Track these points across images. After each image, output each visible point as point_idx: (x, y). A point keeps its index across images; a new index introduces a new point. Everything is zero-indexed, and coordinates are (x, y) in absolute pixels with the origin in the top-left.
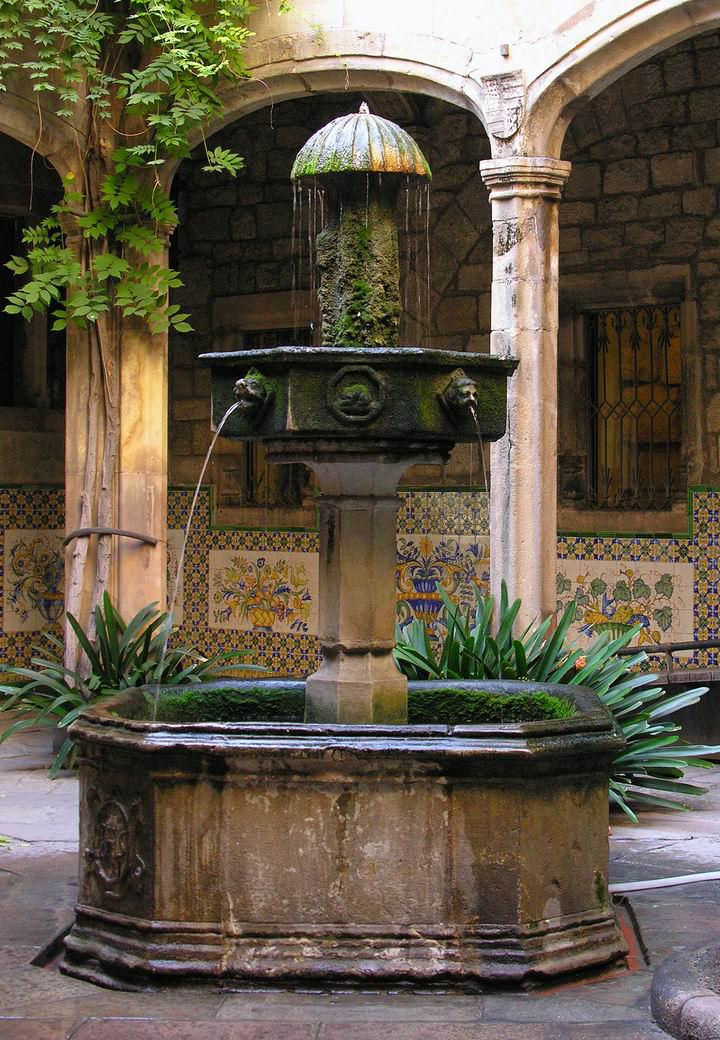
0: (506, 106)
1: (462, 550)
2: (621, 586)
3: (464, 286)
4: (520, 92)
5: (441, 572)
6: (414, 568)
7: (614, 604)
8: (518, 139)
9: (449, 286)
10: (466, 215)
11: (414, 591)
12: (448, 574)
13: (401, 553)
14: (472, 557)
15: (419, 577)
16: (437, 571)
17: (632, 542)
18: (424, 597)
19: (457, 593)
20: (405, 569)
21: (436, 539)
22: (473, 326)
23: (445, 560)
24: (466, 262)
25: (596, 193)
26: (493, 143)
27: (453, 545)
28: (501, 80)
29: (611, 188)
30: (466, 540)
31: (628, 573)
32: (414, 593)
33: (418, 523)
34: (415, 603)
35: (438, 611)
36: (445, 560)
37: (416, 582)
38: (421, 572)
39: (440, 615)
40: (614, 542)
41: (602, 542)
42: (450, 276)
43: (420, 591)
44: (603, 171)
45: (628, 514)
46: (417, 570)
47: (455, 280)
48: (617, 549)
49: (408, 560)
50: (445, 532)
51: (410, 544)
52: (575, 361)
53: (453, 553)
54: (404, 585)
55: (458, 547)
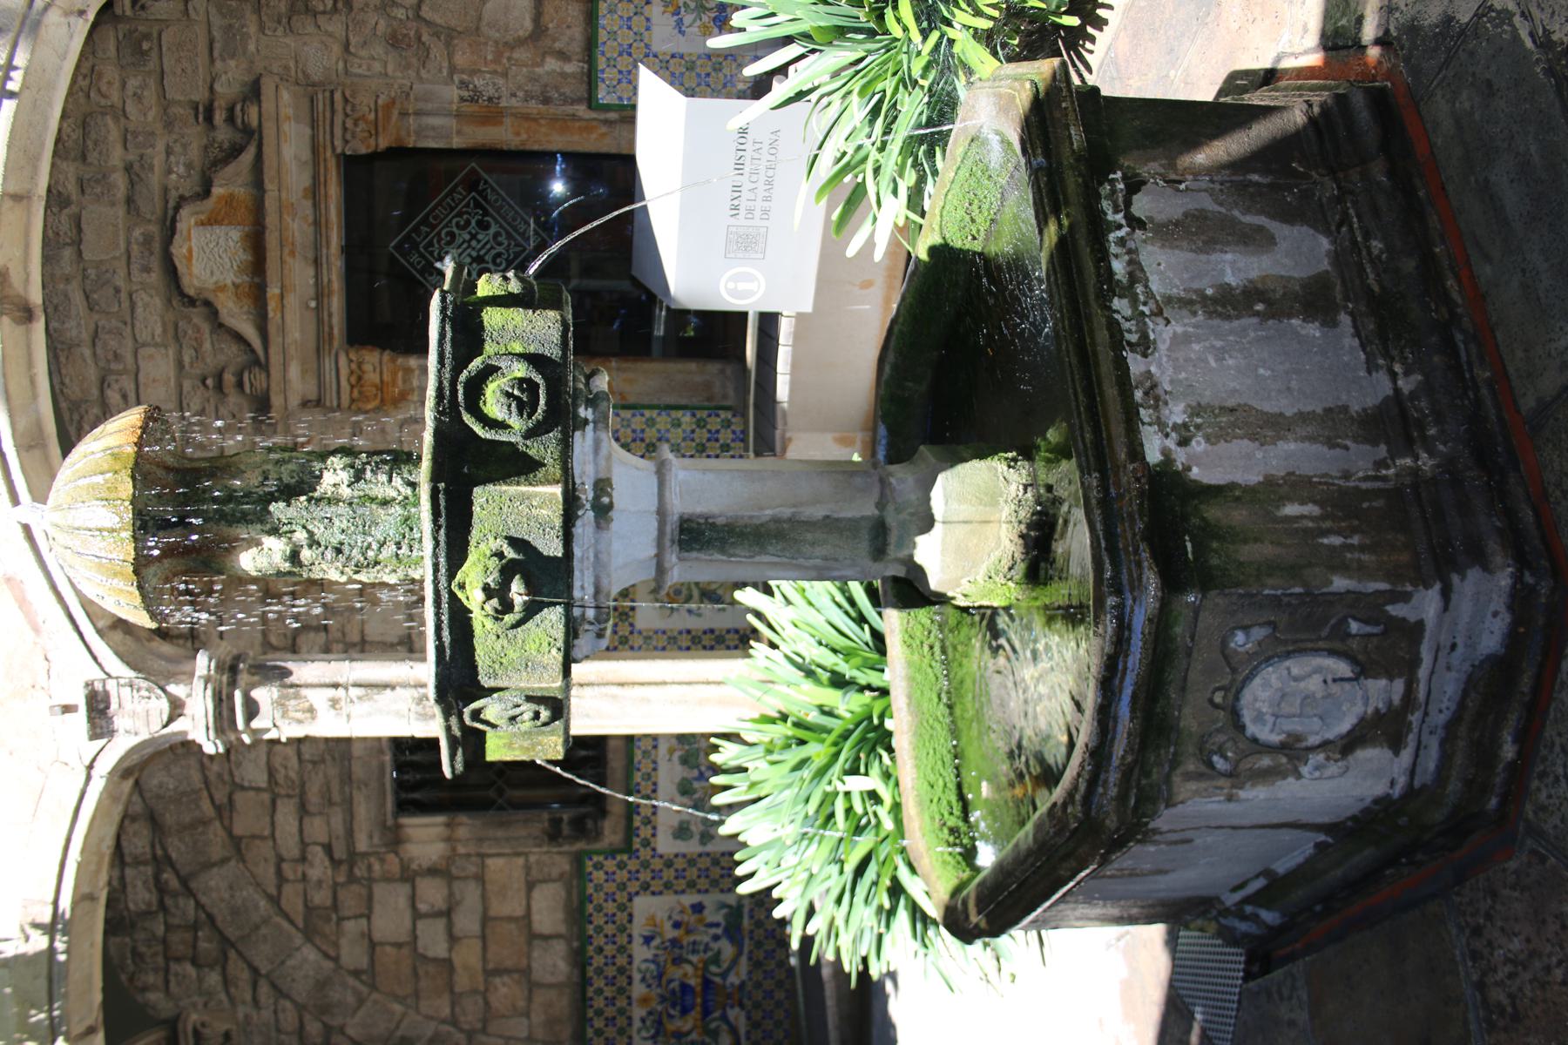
0: (128, 705)
1: (649, 955)
2: (684, 761)
3: (364, 962)
4: (111, 686)
7: (703, 768)
8: (172, 688)
9: (362, 982)
10: (283, 963)
11: (693, 1013)
12: (675, 973)
13: (652, 1031)
15: (678, 1008)
16: (672, 985)
17: (639, 748)
18: (699, 1000)
19: (694, 958)
20: (671, 1026)
21: (638, 990)
22: (406, 951)
23: (660, 976)
24: (336, 959)
25: (266, 797)
26: (175, 727)
28: (98, 709)
29: (261, 779)
30: (641, 953)
31: (671, 751)
32: (695, 1014)
33: (622, 1012)
34: (706, 1012)
35: (713, 982)
37: (685, 1011)
38: (674, 1006)
39: (718, 980)
40: (639, 770)
41: (638, 784)
42: (351, 981)
43: (693, 1007)
44: (243, 788)
45: (610, 756)
46: (672, 1012)
47: (356, 973)
48: (646, 766)
49: (659, 1023)
51: (643, 1020)
52: (448, 825)
53: (652, 967)
55: (646, 961)
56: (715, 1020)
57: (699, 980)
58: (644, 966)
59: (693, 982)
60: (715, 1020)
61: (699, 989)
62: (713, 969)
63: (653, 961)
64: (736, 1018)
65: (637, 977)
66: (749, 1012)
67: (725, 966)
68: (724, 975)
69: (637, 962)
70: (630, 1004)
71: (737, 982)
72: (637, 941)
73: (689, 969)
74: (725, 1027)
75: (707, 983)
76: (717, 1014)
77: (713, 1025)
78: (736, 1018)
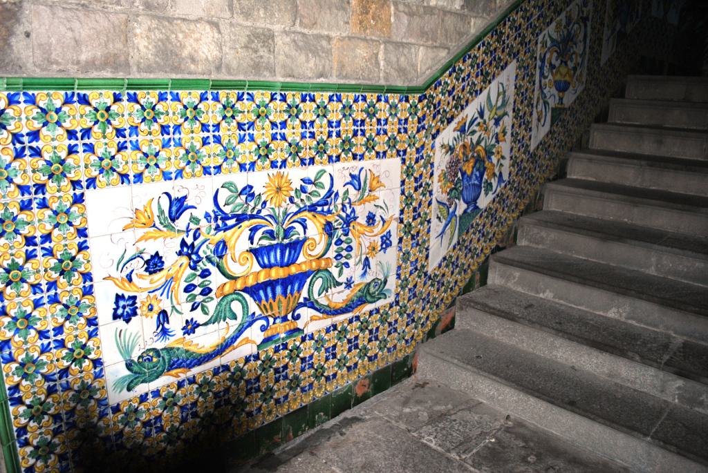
1: (339, 187)
5: (305, 228)
6: (254, 230)
12: (314, 228)
14: (353, 193)
15: (266, 242)
16: (299, 228)
27: (325, 180)
30: (340, 172)
34: (253, 291)
36: (312, 208)
39: (304, 293)
46: (259, 234)
49: (240, 219)
50: (312, 161)
54: (234, 268)
56: (245, 307)
57: (304, 268)
58: (325, 180)
59: (303, 261)
60: (245, 307)
61: (293, 270)
62: (318, 283)
63: (330, 192)
64: (247, 341)
65: (311, 172)
66: (257, 357)
67: (323, 301)
68: (310, 303)
69: (330, 168)
70: (273, 165)
71: (300, 324)
72: (353, 166)
73: (319, 250)
74: (234, 325)
75: (302, 277)
76: (253, 307)
77: (237, 307)
78: (247, 341)
